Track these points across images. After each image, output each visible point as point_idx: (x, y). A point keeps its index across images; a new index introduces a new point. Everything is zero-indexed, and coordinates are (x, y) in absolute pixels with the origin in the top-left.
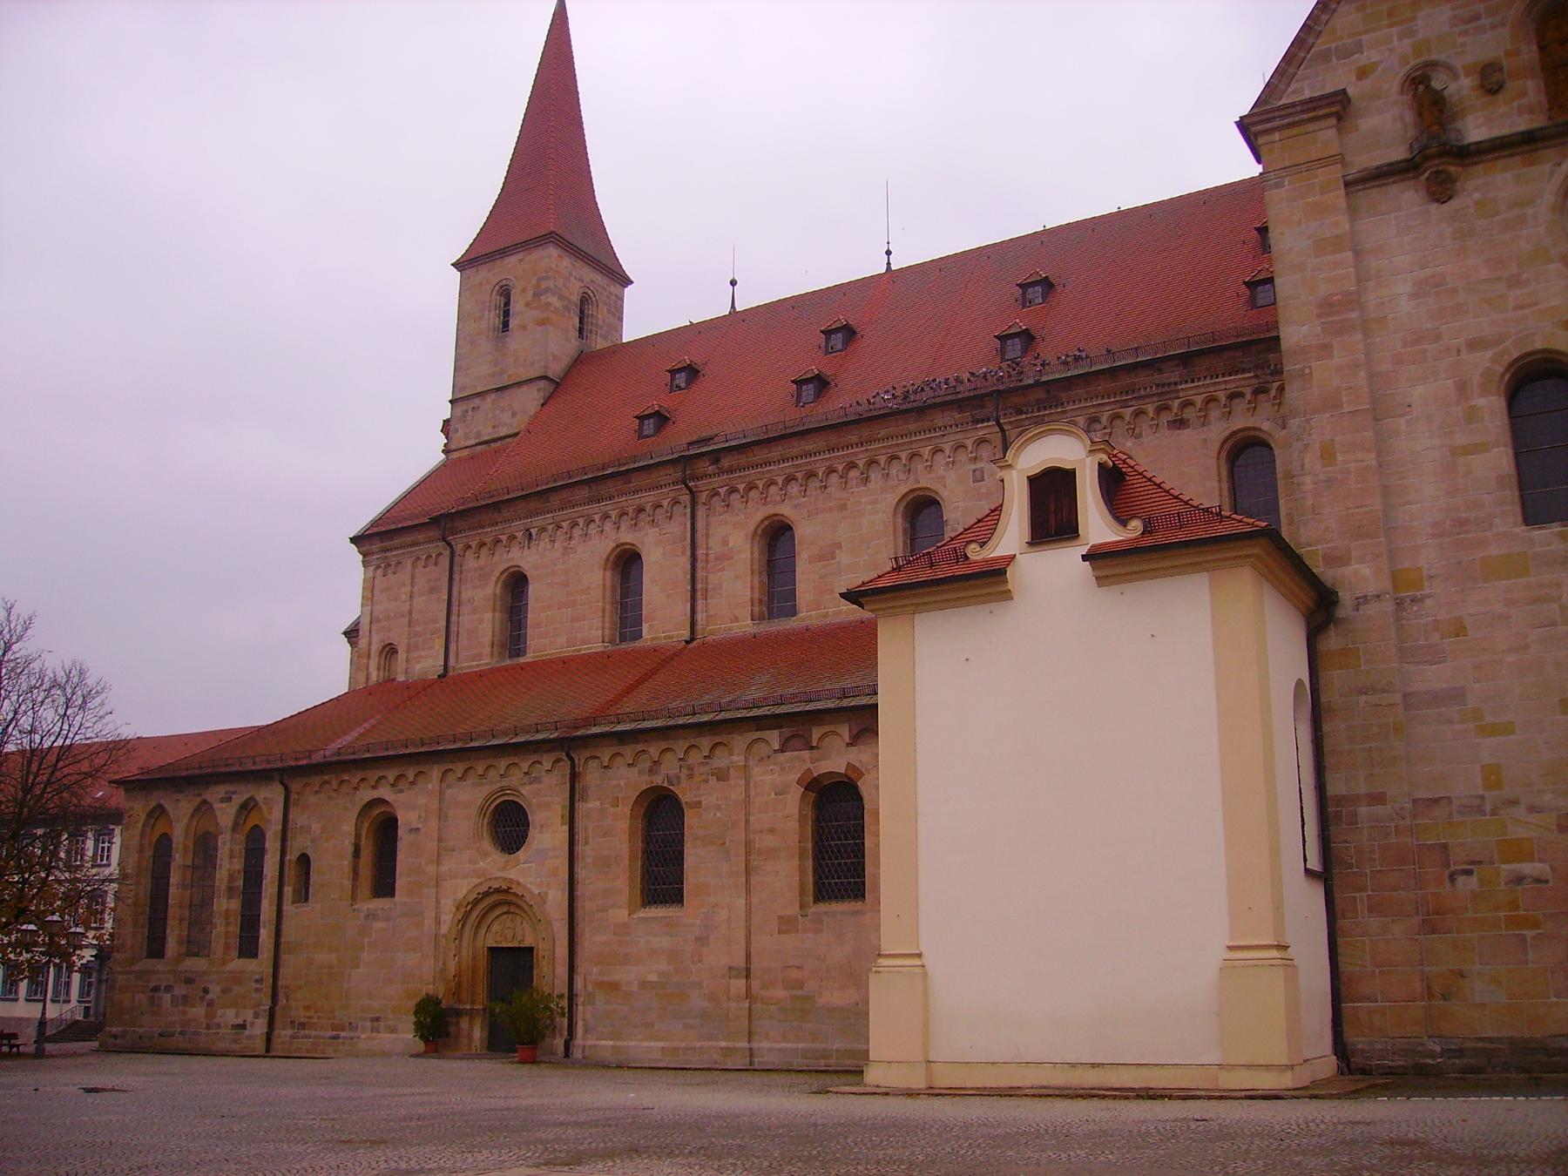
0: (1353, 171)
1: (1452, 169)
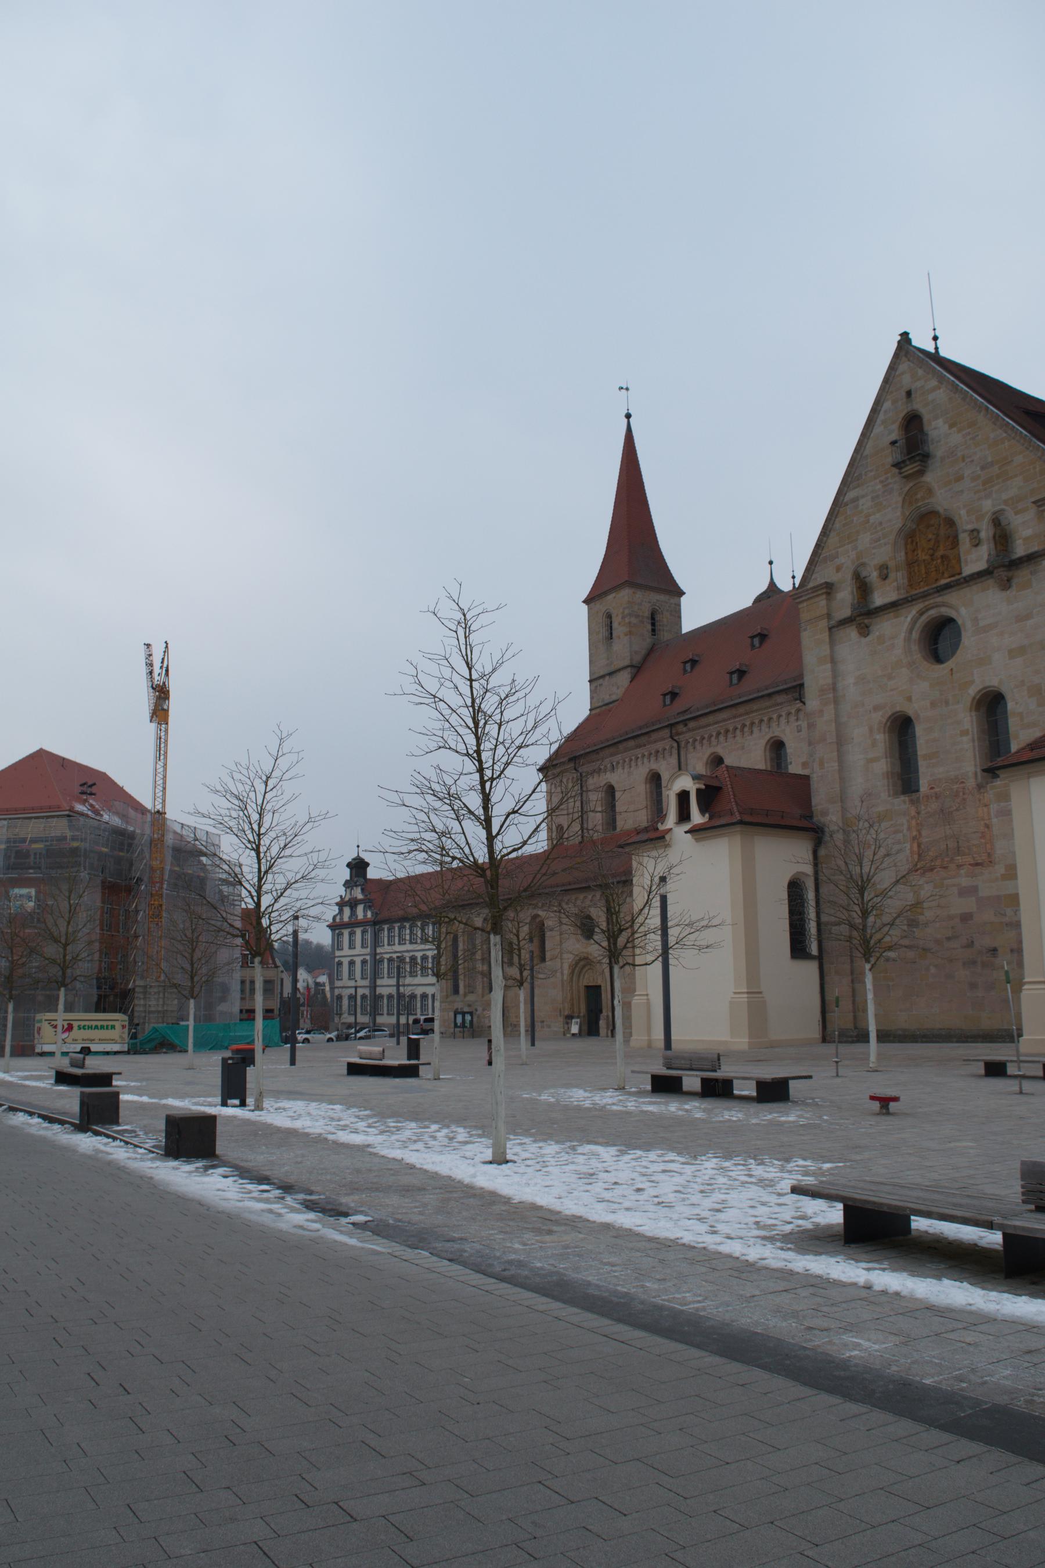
0: (833, 622)
1: (866, 621)
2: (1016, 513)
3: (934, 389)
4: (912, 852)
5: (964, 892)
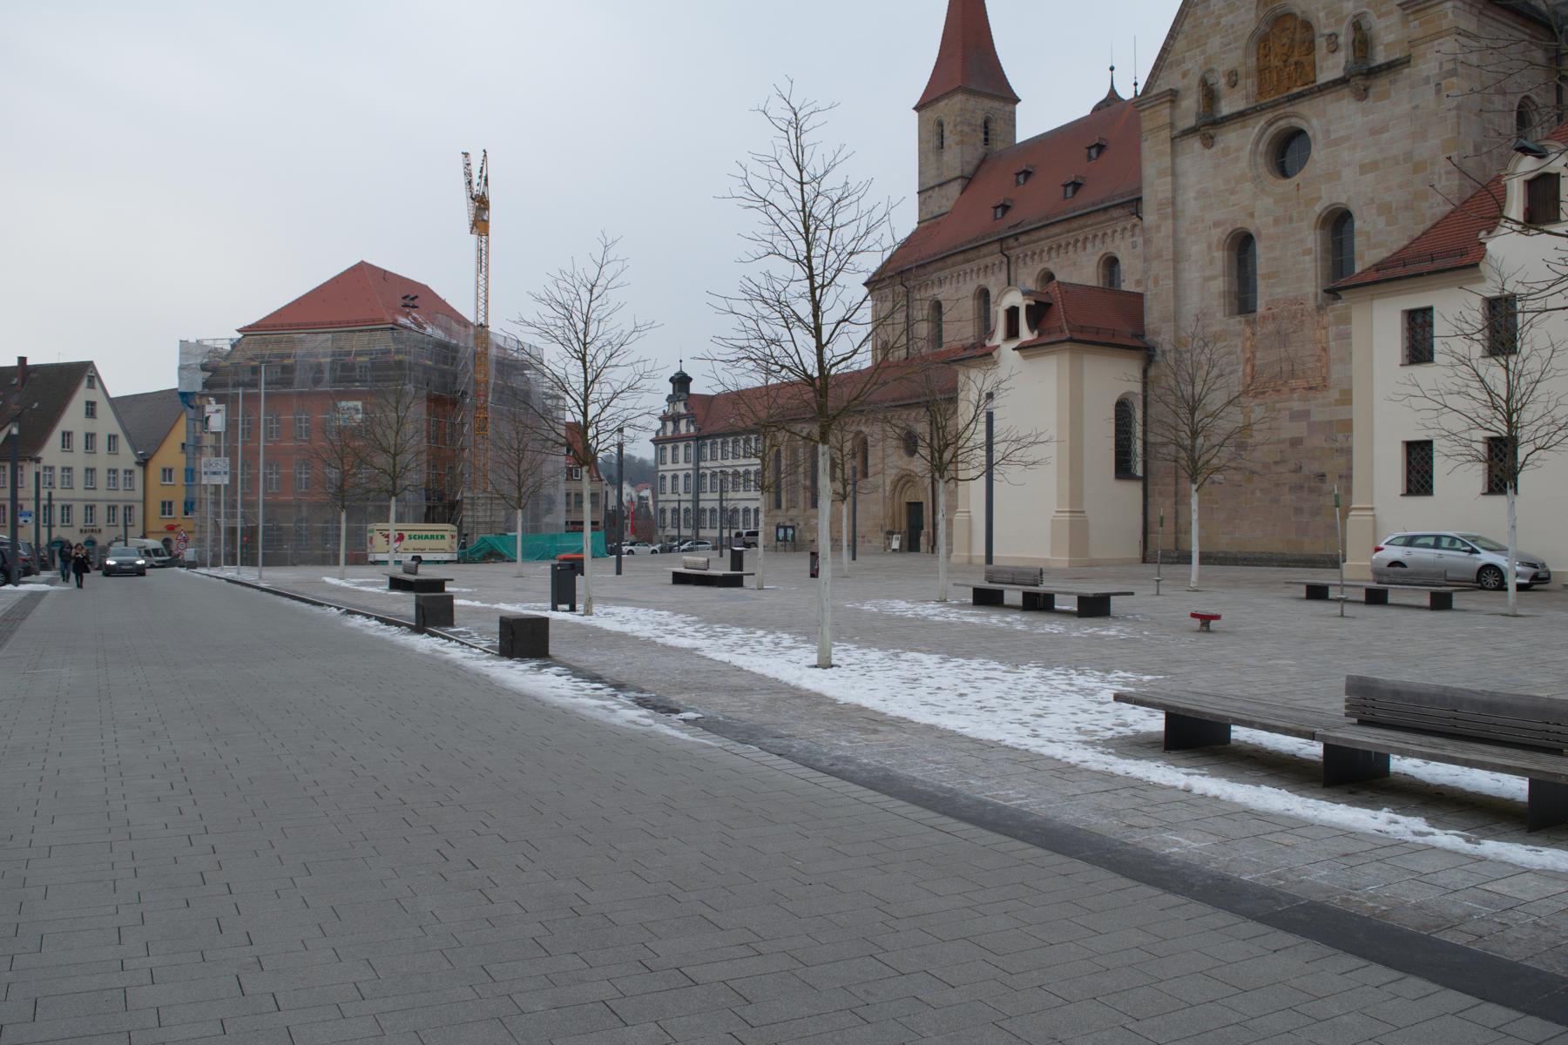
0: (1175, 132)
4: (1244, 374)
5: (1295, 416)
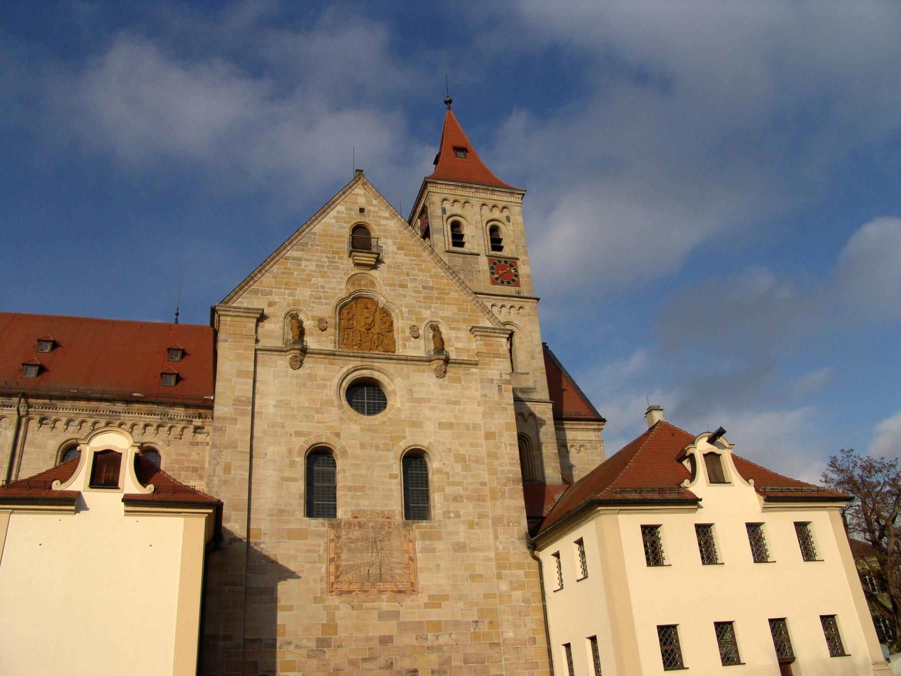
2: (451, 329)
3: (385, 218)
4: (328, 573)
5: (383, 616)
